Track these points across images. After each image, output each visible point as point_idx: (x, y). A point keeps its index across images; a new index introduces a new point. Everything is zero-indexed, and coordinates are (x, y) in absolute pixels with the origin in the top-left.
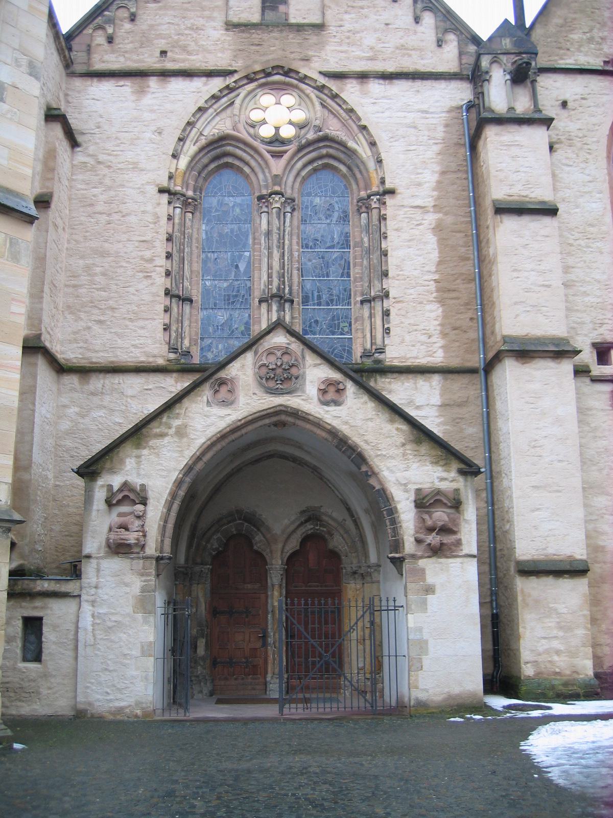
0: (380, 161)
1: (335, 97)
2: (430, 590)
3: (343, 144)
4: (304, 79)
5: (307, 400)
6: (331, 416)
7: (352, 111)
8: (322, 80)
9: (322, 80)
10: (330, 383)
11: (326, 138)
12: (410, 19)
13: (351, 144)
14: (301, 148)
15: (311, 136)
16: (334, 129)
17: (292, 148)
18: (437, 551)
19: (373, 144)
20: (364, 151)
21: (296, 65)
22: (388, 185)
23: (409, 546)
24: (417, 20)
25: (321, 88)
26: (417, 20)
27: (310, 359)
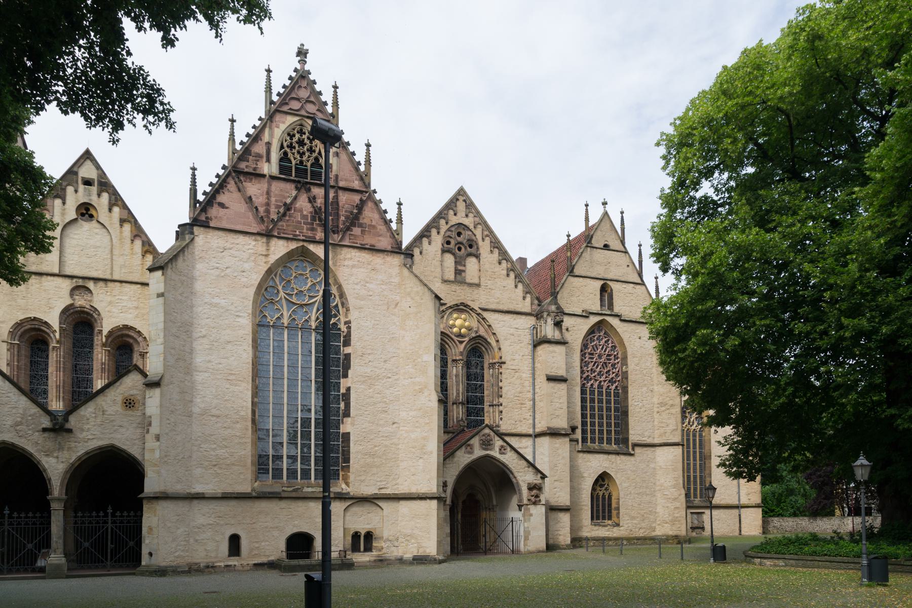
0: (500, 349)
1: (484, 319)
2: (531, 515)
3: (486, 340)
4: (472, 309)
5: (495, 453)
6: (503, 458)
7: (490, 326)
8: (480, 311)
9: (480, 311)
10: (502, 446)
11: (480, 336)
12: (513, 286)
13: (489, 340)
14: (470, 340)
15: (474, 335)
16: (482, 332)
17: (467, 339)
18: (535, 503)
19: (498, 341)
20: (493, 343)
21: (470, 303)
22: (503, 360)
23: (525, 501)
24: (516, 286)
25: (478, 314)
26: (516, 286)
27: (497, 438)
